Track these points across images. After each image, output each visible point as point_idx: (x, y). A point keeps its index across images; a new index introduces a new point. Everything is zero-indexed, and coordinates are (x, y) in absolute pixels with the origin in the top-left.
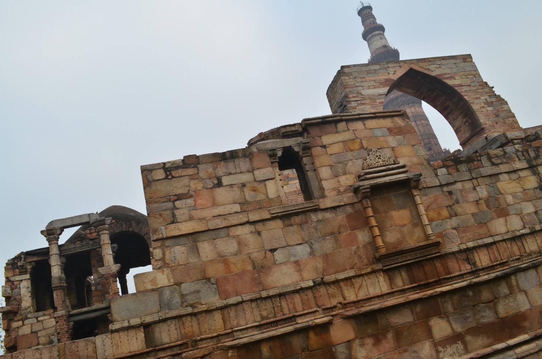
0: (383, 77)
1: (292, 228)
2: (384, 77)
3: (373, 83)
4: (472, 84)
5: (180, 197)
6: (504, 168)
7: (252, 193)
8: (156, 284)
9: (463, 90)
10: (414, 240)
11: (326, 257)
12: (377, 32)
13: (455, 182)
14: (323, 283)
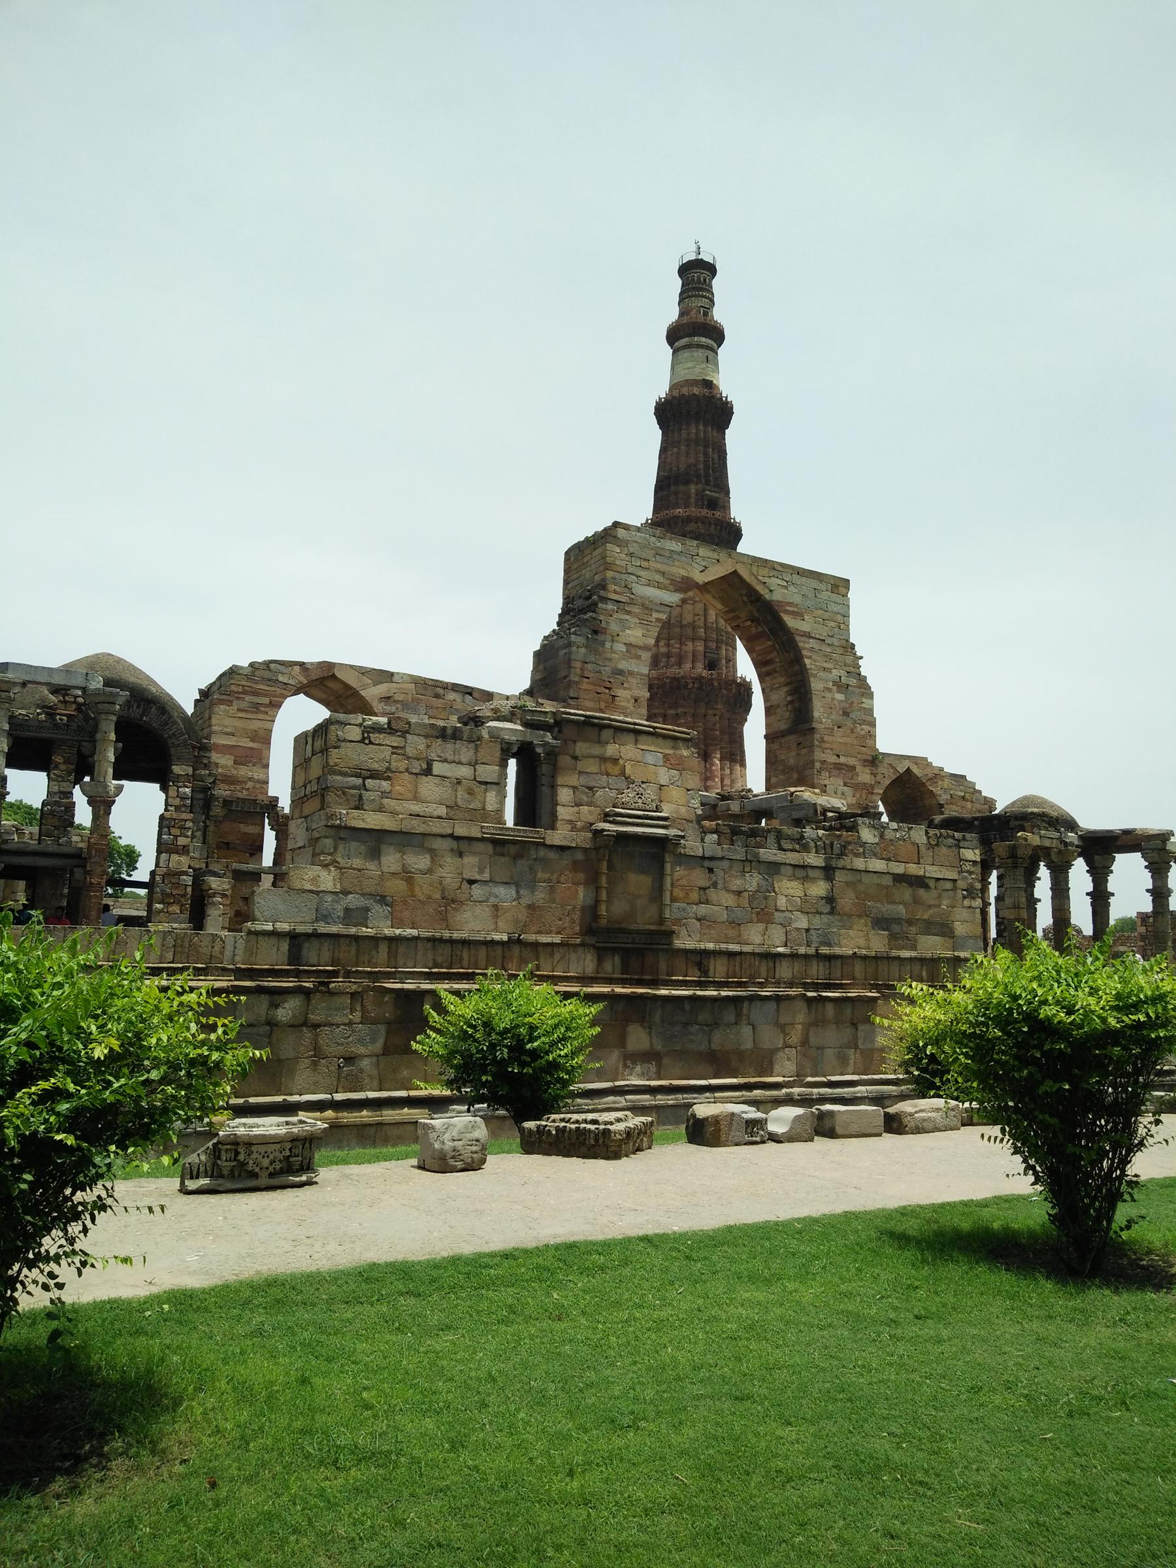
0: (679, 571)
1: (502, 859)
2: (683, 573)
3: (658, 578)
5: (374, 775)
6: (792, 858)
7: (466, 796)
9: (807, 646)
10: (644, 921)
11: (531, 907)
12: (703, 339)
14: (519, 941)
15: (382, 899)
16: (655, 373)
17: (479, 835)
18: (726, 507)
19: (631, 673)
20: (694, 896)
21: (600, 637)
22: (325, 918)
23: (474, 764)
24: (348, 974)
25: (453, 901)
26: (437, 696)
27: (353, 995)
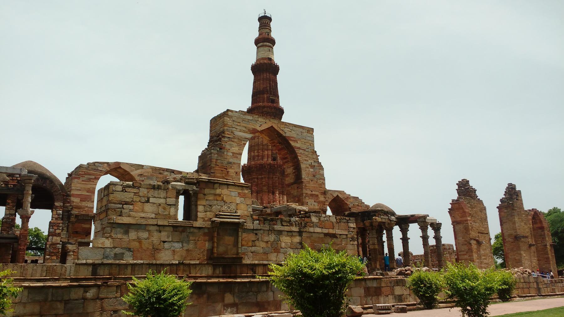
0: (251, 126)
1: (176, 233)
4: (307, 150)
5: (127, 203)
6: (287, 228)
8: (104, 245)
10: (231, 254)
11: (188, 250)
13: (261, 230)
14: (183, 263)
15: (129, 250)
16: (251, 55)
17: (167, 224)
18: (278, 102)
19: (234, 163)
20: (250, 244)
21: (222, 150)
22: (106, 257)
23: (165, 198)
24: (115, 279)
25: (157, 249)
26: (160, 173)
27: (117, 286)
